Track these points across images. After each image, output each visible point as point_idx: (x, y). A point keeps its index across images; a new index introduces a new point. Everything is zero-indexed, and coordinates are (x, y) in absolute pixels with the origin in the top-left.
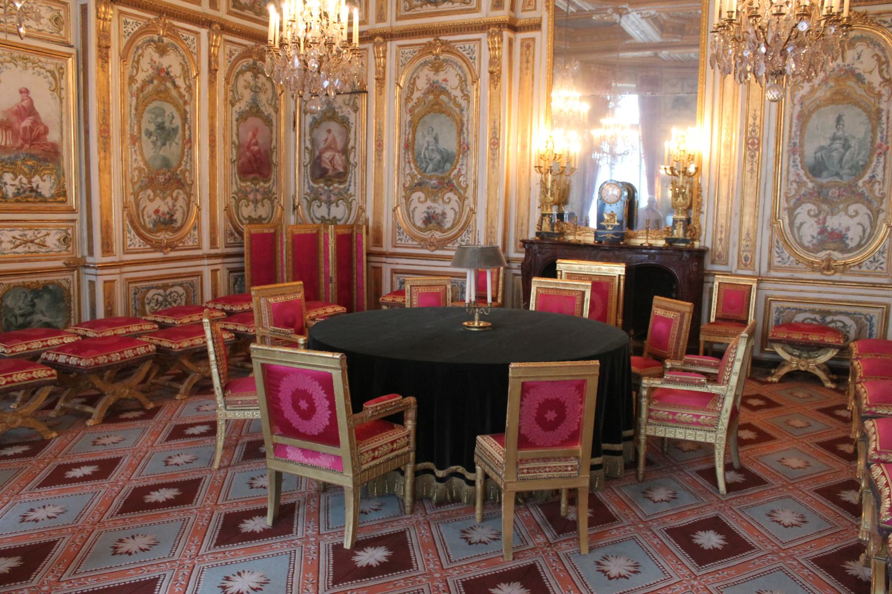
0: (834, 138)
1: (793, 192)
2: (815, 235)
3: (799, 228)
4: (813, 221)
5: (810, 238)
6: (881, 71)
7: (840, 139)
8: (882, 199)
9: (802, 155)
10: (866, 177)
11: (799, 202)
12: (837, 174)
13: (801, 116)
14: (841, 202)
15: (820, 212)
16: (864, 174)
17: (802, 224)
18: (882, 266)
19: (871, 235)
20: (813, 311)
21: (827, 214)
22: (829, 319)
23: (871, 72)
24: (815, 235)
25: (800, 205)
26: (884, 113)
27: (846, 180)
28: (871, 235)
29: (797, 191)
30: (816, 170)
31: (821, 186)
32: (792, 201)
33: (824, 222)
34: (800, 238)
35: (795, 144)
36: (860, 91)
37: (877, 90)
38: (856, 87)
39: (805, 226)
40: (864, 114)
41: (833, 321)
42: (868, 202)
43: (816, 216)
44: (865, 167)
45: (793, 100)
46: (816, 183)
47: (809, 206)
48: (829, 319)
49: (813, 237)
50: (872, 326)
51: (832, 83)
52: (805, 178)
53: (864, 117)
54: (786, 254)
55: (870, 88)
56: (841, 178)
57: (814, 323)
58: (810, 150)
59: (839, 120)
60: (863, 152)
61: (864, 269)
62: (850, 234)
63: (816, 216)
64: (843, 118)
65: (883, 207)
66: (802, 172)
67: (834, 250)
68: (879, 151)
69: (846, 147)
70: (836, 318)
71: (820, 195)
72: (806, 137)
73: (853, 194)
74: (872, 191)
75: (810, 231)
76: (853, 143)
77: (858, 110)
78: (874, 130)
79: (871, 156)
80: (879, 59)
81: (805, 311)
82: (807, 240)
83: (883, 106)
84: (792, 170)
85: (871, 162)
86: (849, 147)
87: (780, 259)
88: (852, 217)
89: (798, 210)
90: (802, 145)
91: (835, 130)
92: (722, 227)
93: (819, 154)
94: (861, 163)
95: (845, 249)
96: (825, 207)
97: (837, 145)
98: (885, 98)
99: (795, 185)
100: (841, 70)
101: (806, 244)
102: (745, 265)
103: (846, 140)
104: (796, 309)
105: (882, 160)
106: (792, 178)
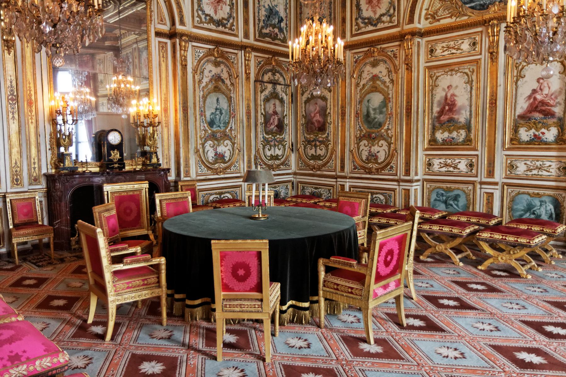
0: (216, 109)
1: (203, 135)
2: (213, 156)
3: (207, 153)
4: (211, 149)
5: (211, 158)
6: (230, 79)
7: (219, 109)
8: (235, 137)
9: (205, 117)
10: (229, 128)
11: (206, 141)
12: (219, 126)
13: (203, 97)
14: (222, 140)
15: (214, 145)
16: (228, 126)
17: (208, 151)
18: (238, 168)
19: (233, 154)
20: (216, 194)
21: (217, 146)
22: (222, 196)
23: (227, 79)
24: (213, 156)
25: (206, 142)
26: (232, 99)
27: (223, 129)
28: (233, 154)
29: (205, 135)
30: (211, 123)
31: (214, 132)
32: (203, 140)
33: (216, 150)
34: (208, 158)
35: (202, 111)
36: (224, 87)
37: (230, 87)
38: (222, 85)
39: (209, 152)
40: (226, 98)
41: (224, 197)
42: (230, 139)
43: (213, 147)
44: (228, 123)
45: (199, 88)
46: (212, 131)
47: (210, 142)
48: (222, 196)
49: (213, 157)
50: (237, 196)
51: (213, 82)
52: (207, 128)
53: (226, 100)
54: (203, 167)
55: (227, 87)
56: (221, 128)
57: (217, 199)
58: (208, 114)
59: (218, 100)
60: (227, 116)
61: (232, 170)
62: (226, 155)
63: (213, 147)
64: (219, 99)
65: (236, 141)
66: (206, 125)
67: (221, 163)
68: (232, 116)
69: (221, 113)
70: (225, 195)
71: (213, 137)
72: (206, 108)
73: (226, 136)
74: (231, 134)
75: (211, 155)
76: (223, 112)
77: (224, 96)
78: (230, 106)
79: (230, 118)
80: (229, 74)
81: (213, 194)
82: (210, 159)
83: (232, 95)
84: (202, 124)
85: (230, 120)
86: (222, 113)
87: (200, 170)
88: (226, 146)
89: (206, 144)
90: (205, 112)
91: (216, 105)
92: (167, 155)
93: (211, 116)
94: (227, 121)
95: (225, 162)
96: (216, 142)
97: (218, 112)
98: (232, 92)
99: (203, 132)
100: (216, 76)
101: (211, 161)
102: (187, 175)
103: (221, 110)
104: (209, 194)
105: (234, 120)
106: (202, 128)
